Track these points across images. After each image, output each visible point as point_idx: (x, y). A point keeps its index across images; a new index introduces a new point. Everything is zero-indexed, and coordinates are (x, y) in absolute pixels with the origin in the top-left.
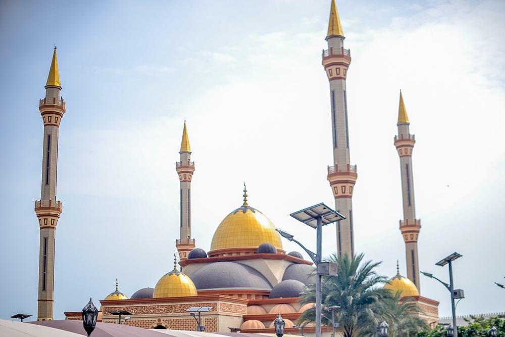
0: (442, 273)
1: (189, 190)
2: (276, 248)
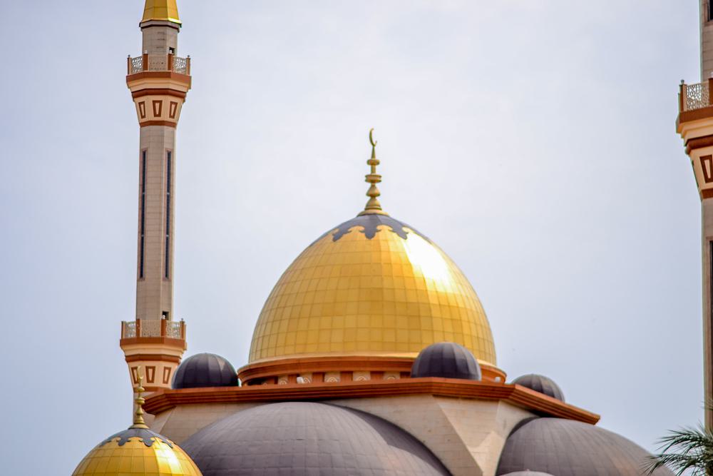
1: (170, 155)
2: (480, 362)
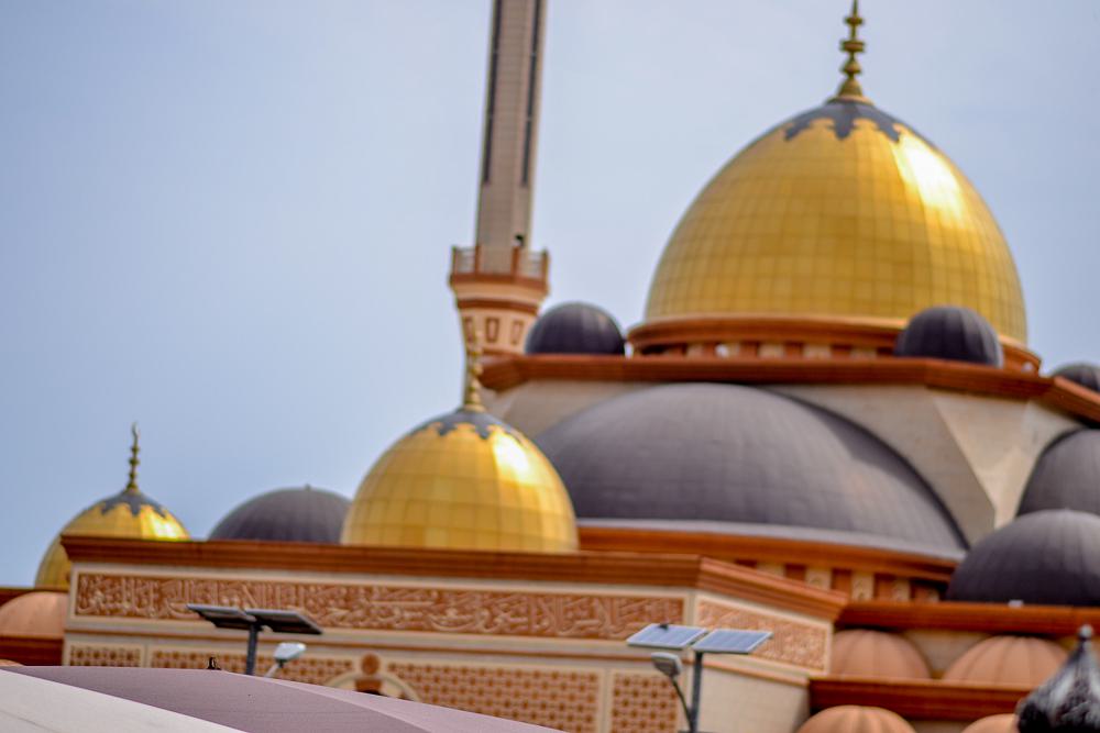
2: (1003, 339)
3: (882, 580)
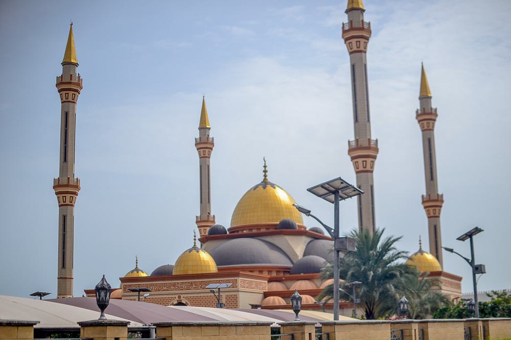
0: (464, 248)
1: (208, 166)
2: (297, 224)
3: (278, 272)
